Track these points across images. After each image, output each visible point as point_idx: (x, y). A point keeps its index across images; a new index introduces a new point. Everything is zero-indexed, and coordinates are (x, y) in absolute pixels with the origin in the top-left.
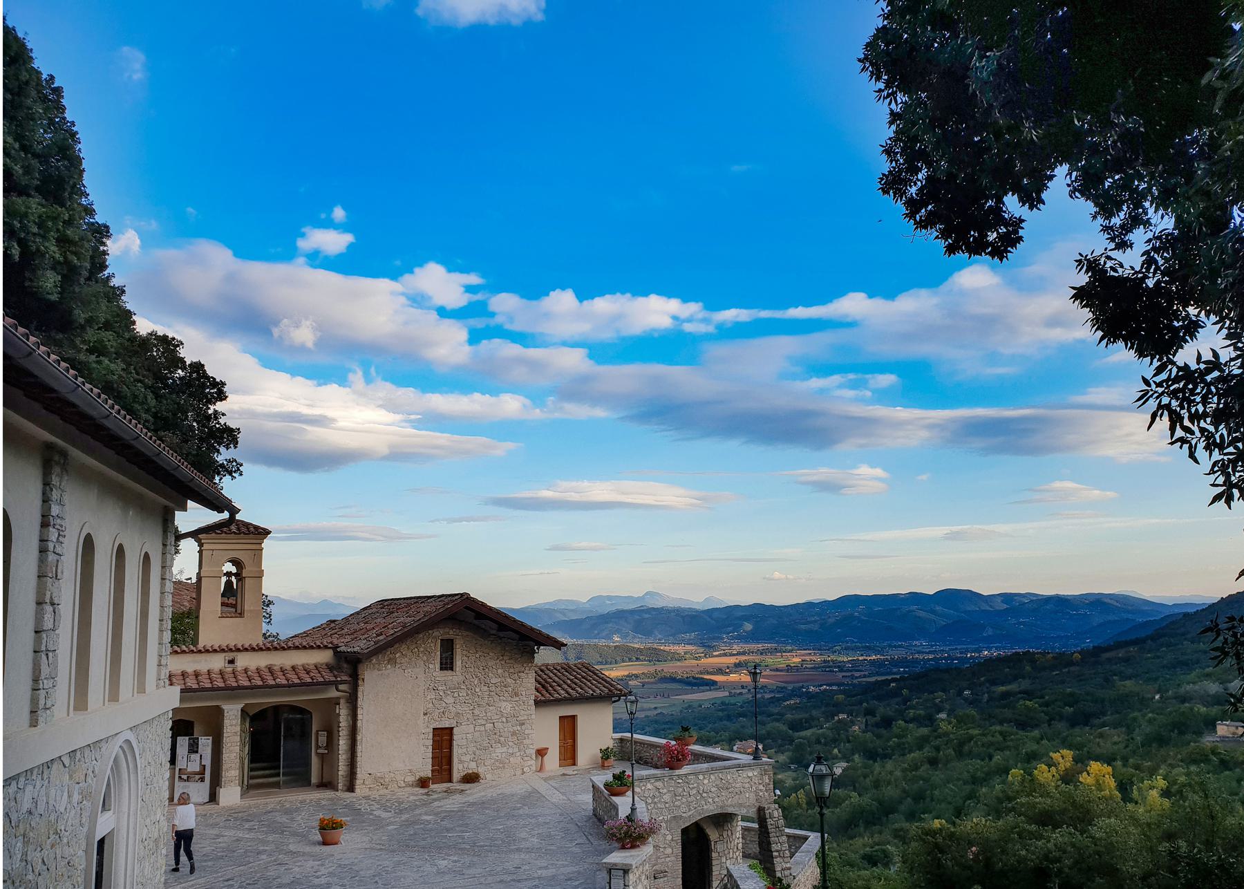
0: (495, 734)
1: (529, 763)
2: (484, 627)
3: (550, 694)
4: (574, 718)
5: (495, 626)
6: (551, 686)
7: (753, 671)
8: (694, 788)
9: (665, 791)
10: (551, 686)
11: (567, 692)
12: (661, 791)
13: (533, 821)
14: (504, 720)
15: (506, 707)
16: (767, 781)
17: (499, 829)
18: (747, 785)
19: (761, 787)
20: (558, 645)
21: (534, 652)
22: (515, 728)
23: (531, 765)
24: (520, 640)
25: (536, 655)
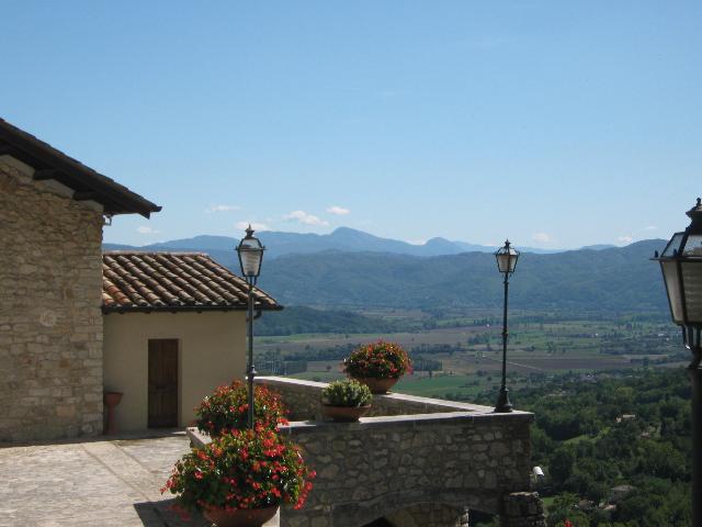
0: (29, 362)
1: (92, 417)
2: (7, 170)
3: (131, 298)
4: (174, 343)
5: (29, 170)
6: (137, 288)
7: (503, 251)
8: (381, 456)
9: (327, 459)
10: (137, 288)
11: (164, 298)
12: (320, 458)
13: (77, 503)
14: (46, 340)
15: (49, 318)
16: (520, 450)
17: (8, 514)
18: (483, 456)
19: (507, 461)
20: (146, 208)
21: (103, 223)
22: (66, 355)
23: (96, 421)
24: (76, 198)
25: (104, 228)
